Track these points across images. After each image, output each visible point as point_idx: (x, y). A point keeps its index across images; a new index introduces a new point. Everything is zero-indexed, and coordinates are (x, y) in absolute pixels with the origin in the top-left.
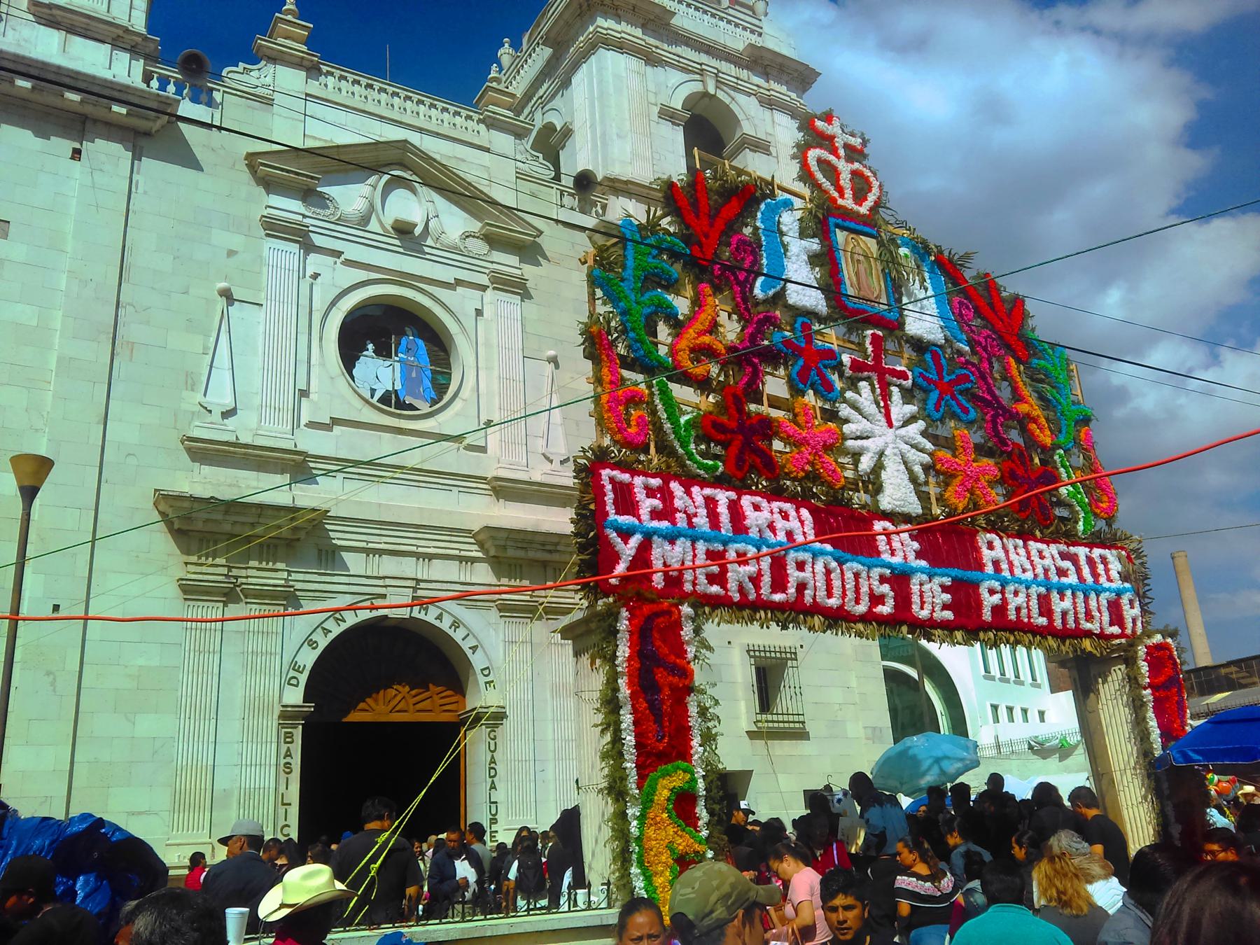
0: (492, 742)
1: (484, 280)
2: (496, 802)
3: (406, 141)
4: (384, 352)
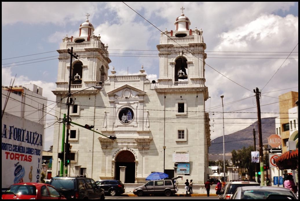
1: (138, 102)
4: (125, 115)
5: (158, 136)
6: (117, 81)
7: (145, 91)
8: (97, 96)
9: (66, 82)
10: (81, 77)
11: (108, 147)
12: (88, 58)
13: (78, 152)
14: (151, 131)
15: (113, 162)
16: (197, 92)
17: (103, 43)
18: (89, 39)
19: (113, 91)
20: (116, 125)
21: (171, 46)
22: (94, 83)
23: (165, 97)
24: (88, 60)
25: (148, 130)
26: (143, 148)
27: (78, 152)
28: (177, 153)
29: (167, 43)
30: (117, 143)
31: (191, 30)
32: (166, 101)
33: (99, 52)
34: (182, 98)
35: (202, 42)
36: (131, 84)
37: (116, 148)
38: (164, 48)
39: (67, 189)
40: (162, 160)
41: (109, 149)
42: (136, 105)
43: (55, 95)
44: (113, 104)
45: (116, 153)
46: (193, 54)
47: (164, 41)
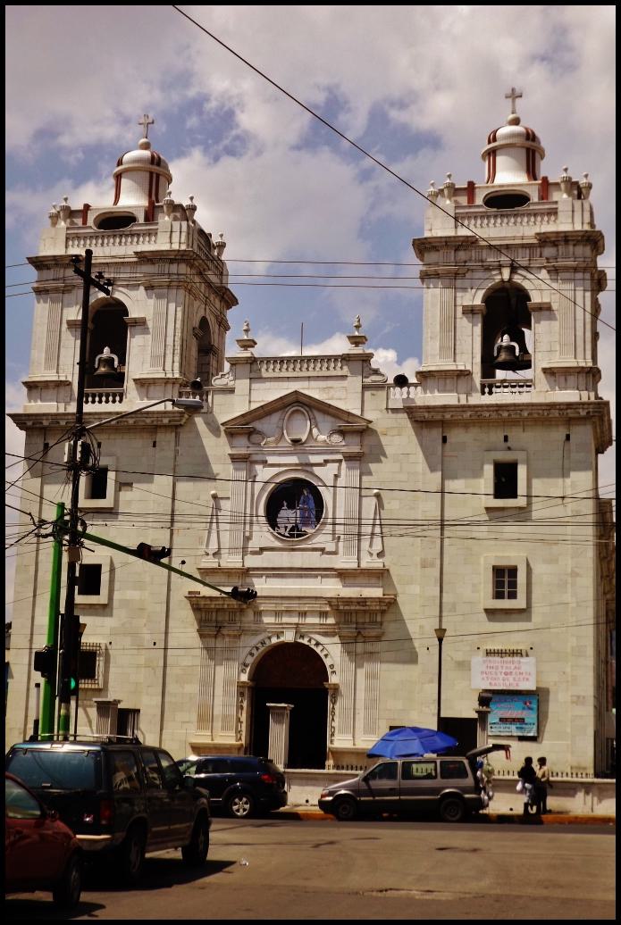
1: (340, 457)
3: (296, 392)
4: (291, 507)
5: (416, 589)
6: (260, 379)
7: (368, 416)
8: (184, 435)
9: (63, 379)
10: (122, 362)
11: (225, 631)
12: (146, 289)
13: (106, 649)
14: (388, 570)
16: (569, 422)
17: (207, 231)
18: (151, 215)
19: (243, 415)
20: (254, 544)
21: (469, 243)
22: (170, 386)
23: (444, 440)
24: (150, 297)
25: (377, 564)
26: (359, 633)
27: (106, 649)
28: (489, 653)
29: (451, 233)
30: (259, 614)
31: (545, 179)
32: (446, 454)
33: (192, 266)
34: (509, 444)
35: (587, 228)
36: (314, 391)
37: (256, 633)
38: (441, 252)
39: (70, 789)
40: (431, 681)
41: (229, 635)
42: (332, 468)
43: (21, 429)
44: (243, 465)
45: (254, 651)
46: (555, 271)
47: (440, 227)
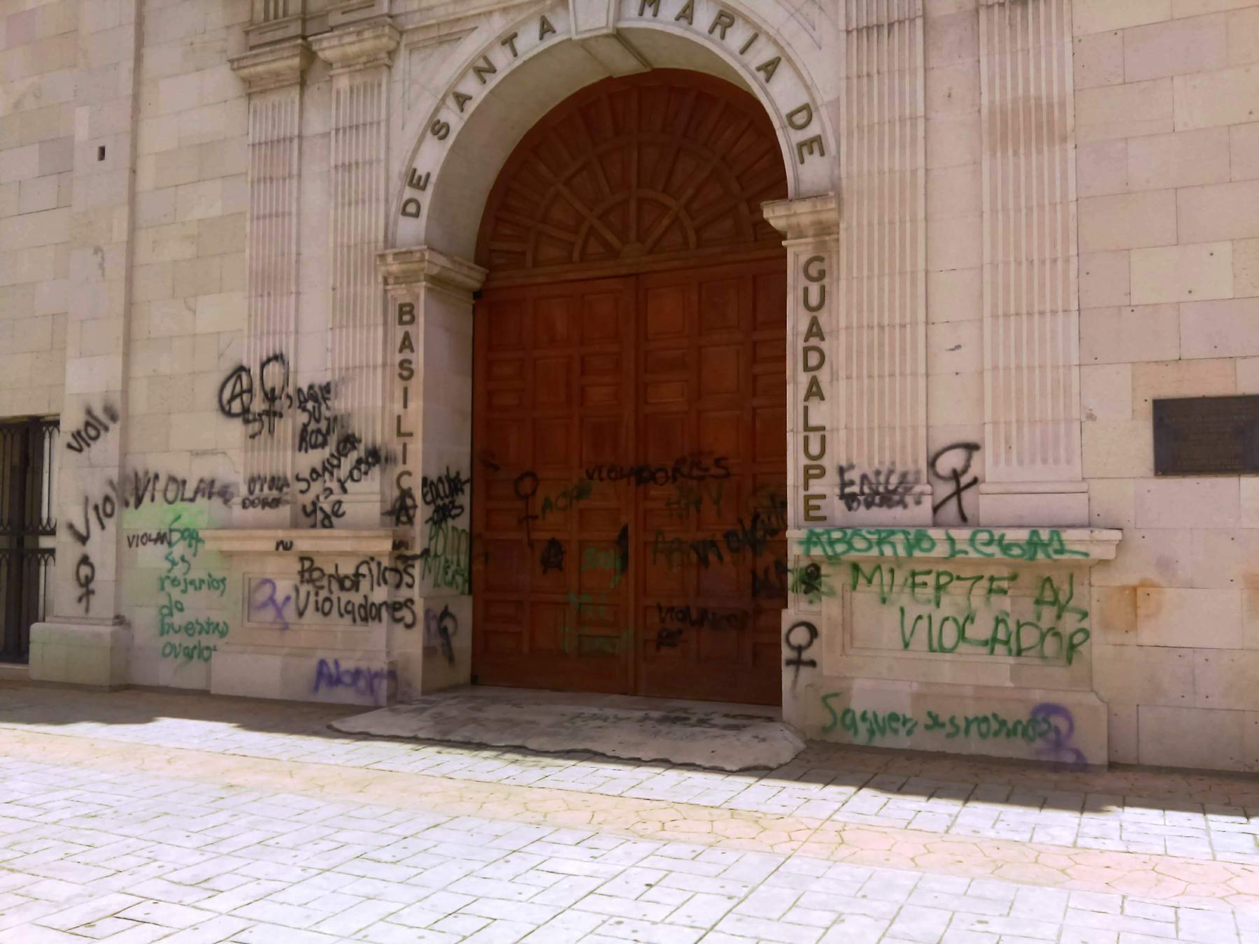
0: (814, 289)
2: (823, 428)
15: (405, 279)
